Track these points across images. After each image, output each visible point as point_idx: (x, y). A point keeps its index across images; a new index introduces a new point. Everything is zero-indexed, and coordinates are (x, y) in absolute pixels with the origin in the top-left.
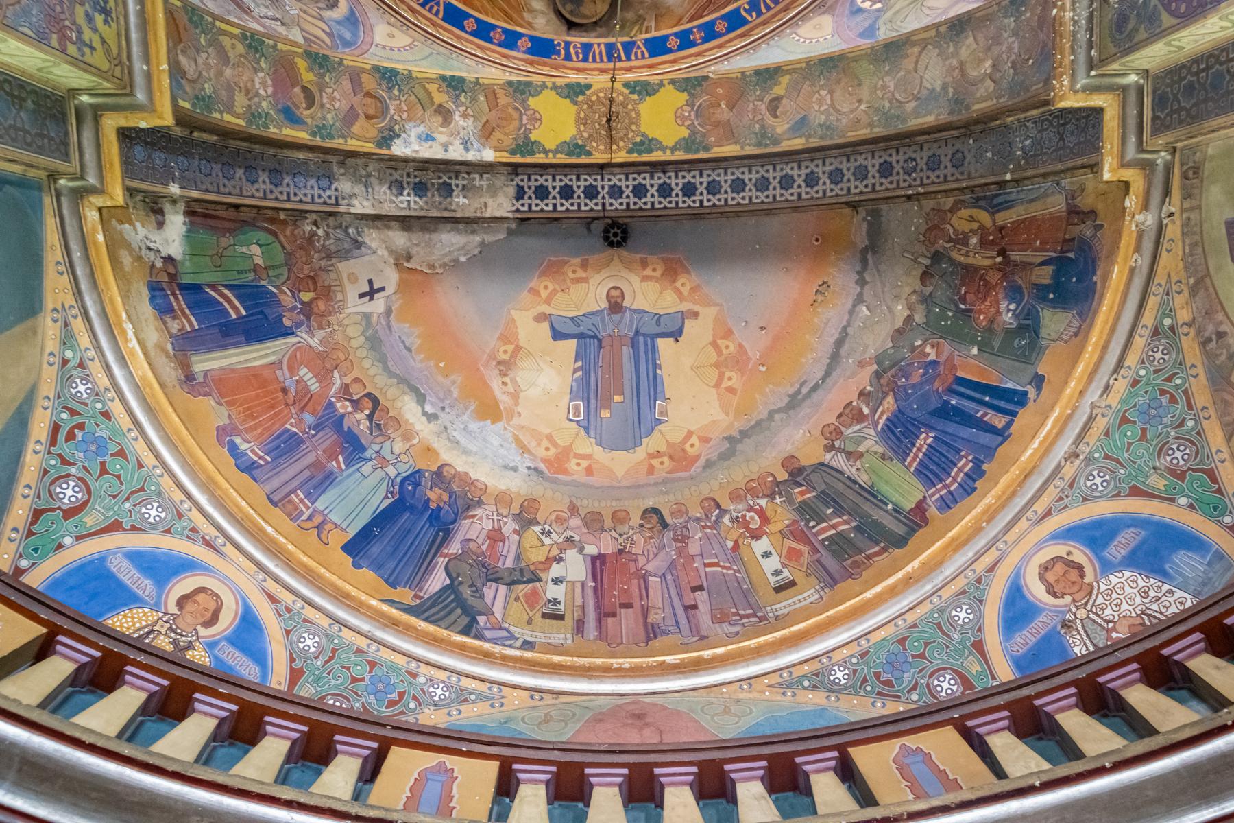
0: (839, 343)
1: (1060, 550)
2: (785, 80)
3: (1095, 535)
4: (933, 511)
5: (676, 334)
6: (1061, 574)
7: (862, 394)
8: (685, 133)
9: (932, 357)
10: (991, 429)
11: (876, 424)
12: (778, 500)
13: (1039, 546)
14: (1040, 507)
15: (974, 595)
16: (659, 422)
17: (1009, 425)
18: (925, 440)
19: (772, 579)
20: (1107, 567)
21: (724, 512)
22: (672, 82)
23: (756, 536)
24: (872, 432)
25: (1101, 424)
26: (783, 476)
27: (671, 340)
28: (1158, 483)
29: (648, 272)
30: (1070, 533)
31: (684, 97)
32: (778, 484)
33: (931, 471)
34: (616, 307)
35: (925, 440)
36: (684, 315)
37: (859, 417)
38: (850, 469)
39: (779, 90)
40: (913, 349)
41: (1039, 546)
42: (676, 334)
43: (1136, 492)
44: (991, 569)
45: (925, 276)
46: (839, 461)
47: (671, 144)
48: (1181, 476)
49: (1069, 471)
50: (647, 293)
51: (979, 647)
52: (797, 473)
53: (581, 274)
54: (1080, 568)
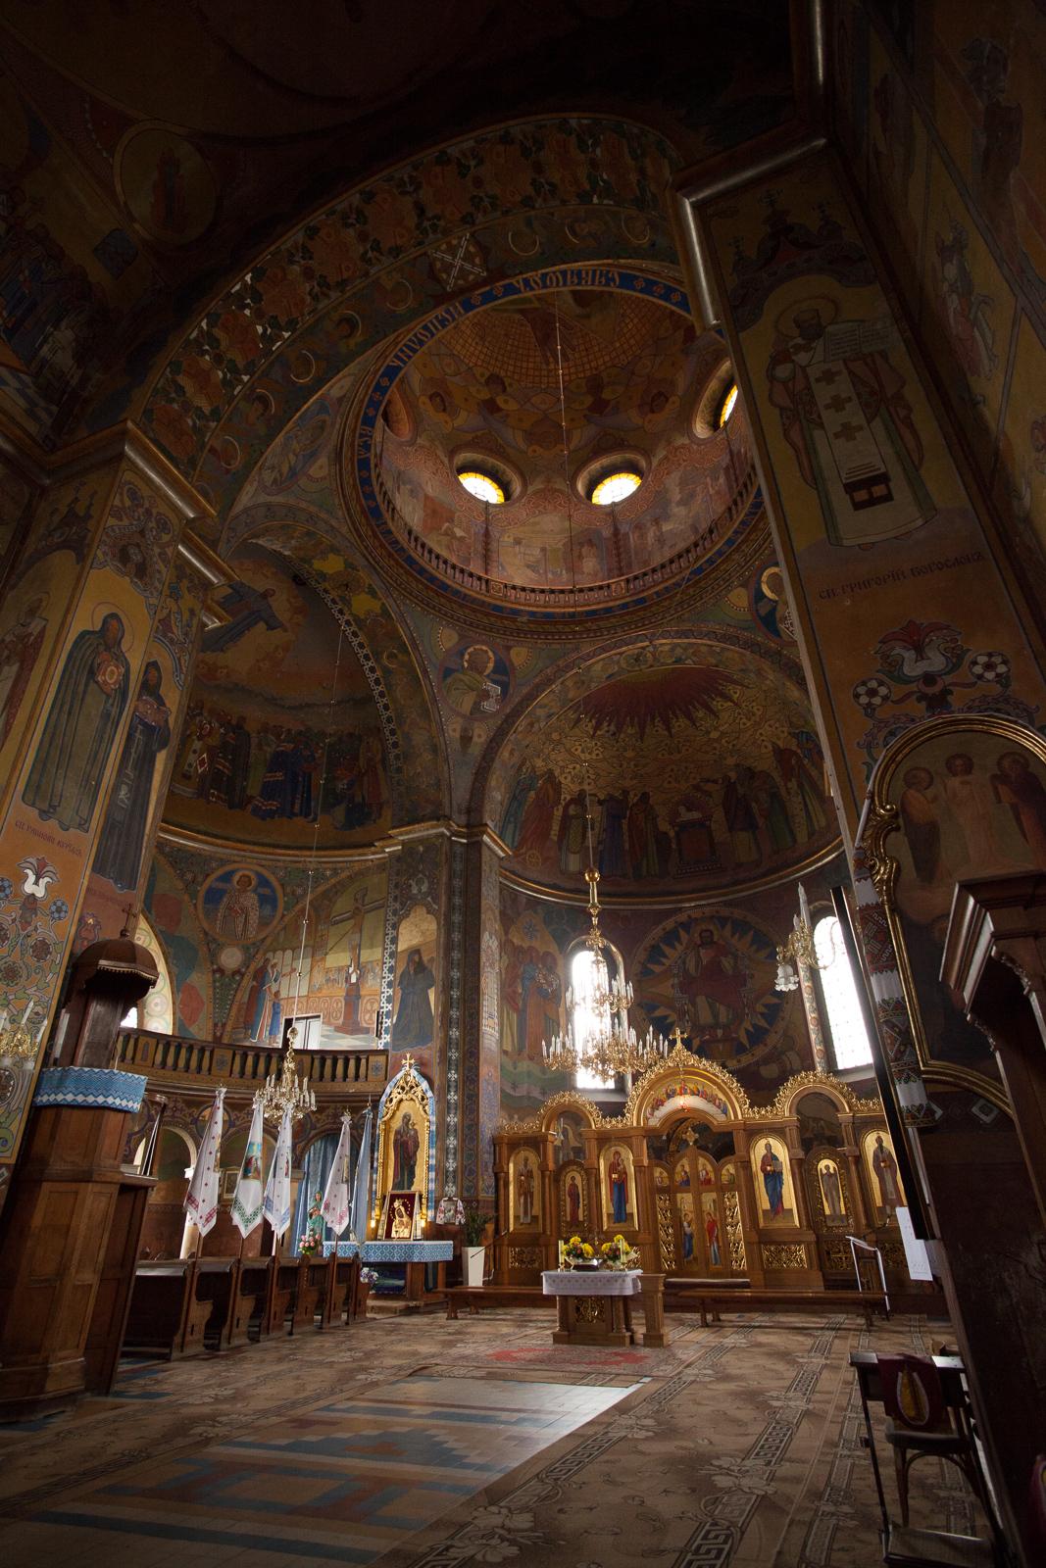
0: (308, 705)
1: (253, 876)
2: (406, 659)
3: (264, 882)
4: (250, 807)
5: (270, 628)
6: (245, 881)
7: (289, 730)
8: (363, 617)
9: (317, 755)
10: (293, 805)
11: (278, 746)
12: (222, 731)
13: (251, 870)
14: (264, 863)
15: (223, 862)
16: (222, 650)
17: (296, 815)
18: (279, 776)
19: (186, 768)
20: (255, 891)
21: (201, 714)
22: (383, 604)
23: (200, 738)
24: (274, 746)
25: (300, 865)
26: (234, 722)
27: (265, 627)
28: (288, 890)
29: (293, 600)
30: (259, 875)
31: (380, 611)
32: (229, 722)
33: (268, 791)
34: (265, 595)
35: (279, 776)
36: (282, 626)
37: (278, 736)
38: (253, 751)
39: (400, 656)
40: (317, 744)
41: (251, 870)
42: (270, 628)
43: (282, 885)
44: (235, 862)
45: (351, 735)
46: (254, 741)
47: (354, 612)
48: (293, 894)
49: (279, 864)
50: (282, 604)
51: (208, 875)
52: (238, 728)
53: (269, 574)
54: (250, 884)
